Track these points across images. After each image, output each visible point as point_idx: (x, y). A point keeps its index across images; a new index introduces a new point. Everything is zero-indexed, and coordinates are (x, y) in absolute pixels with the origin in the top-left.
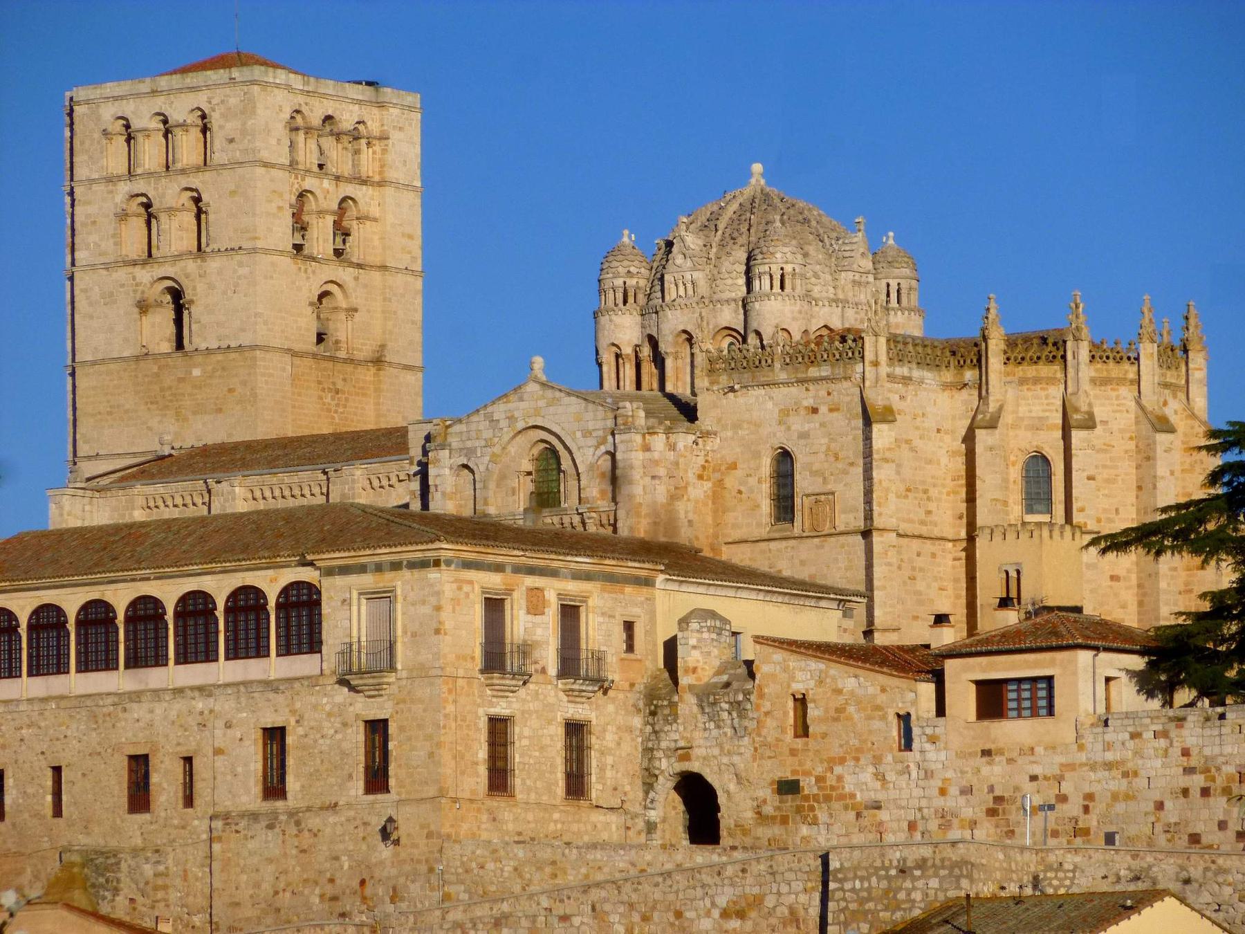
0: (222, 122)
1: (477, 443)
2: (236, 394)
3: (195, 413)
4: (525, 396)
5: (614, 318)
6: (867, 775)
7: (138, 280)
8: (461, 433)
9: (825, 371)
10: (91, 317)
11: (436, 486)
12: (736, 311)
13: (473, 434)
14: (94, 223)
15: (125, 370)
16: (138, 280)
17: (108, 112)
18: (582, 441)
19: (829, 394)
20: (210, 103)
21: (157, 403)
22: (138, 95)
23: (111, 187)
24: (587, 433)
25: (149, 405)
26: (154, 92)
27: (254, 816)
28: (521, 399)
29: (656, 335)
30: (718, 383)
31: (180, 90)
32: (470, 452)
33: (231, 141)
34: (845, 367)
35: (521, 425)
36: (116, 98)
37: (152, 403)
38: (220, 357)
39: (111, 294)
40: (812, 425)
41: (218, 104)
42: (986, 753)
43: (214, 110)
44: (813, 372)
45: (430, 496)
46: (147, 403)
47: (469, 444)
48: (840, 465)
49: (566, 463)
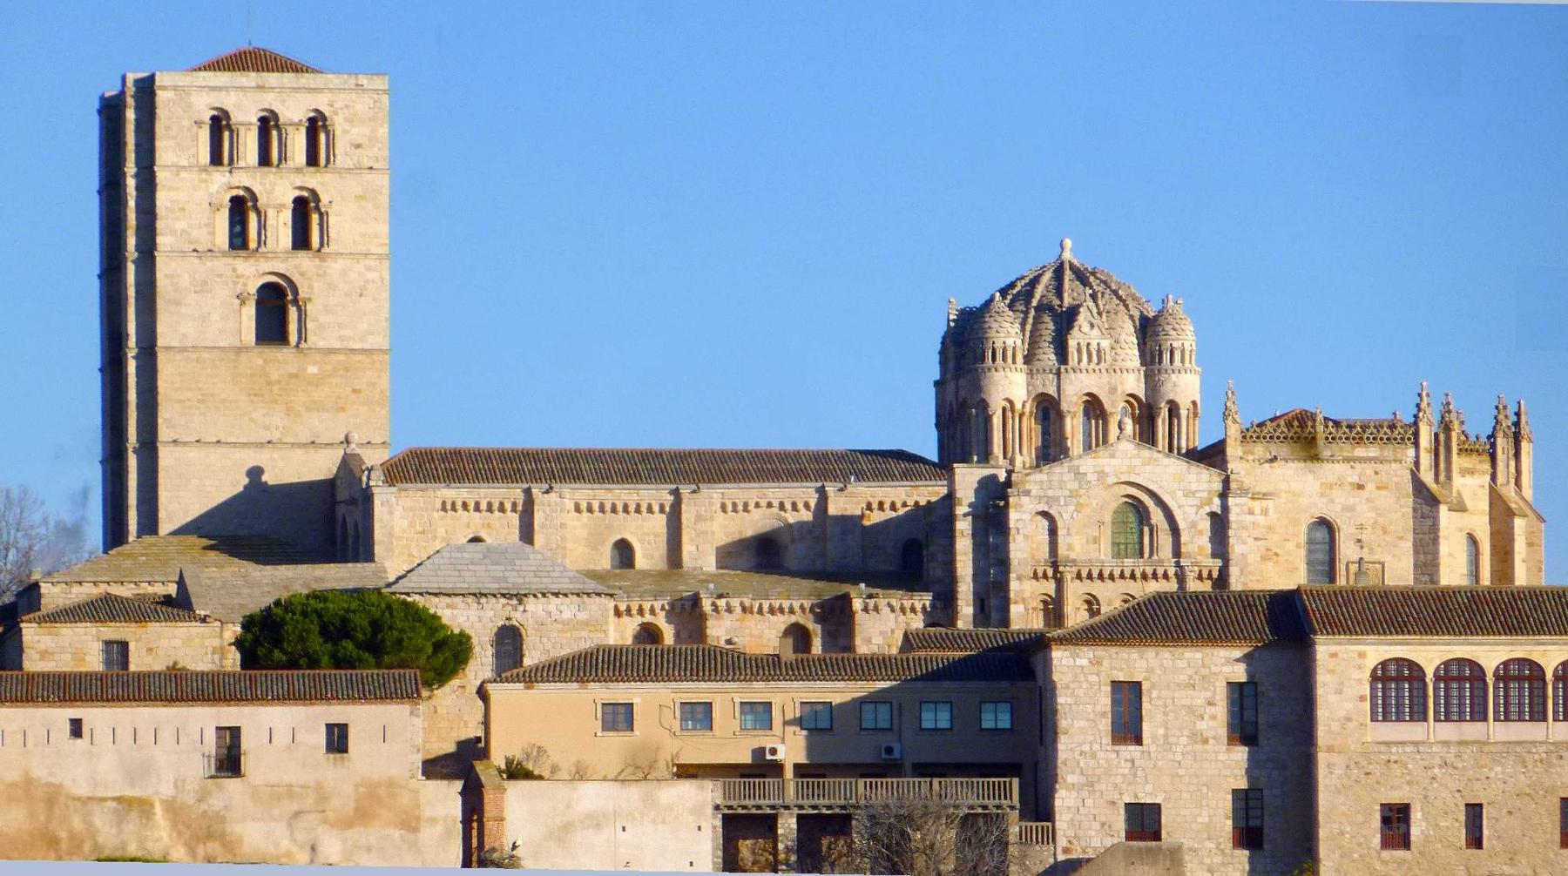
1: (1060, 493)
3: (308, 409)
5: (1009, 374)
7: (239, 272)
8: (1042, 482)
9: (1373, 451)
11: (1018, 529)
12: (1138, 380)
13: (1055, 484)
14: (183, 209)
15: (222, 360)
16: (239, 272)
18: (1183, 501)
19: (1376, 473)
20: (332, 106)
21: (262, 395)
22: (242, 88)
23: (204, 176)
24: (1188, 493)
25: (252, 398)
26: (260, 88)
28: (1112, 456)
29: (1056, 396)
30: (1252, 453)
31: (296, 89)
32: (1051, 500)
33: (358, 146)
34: (1394, 450)
36: (213, 89)
37: (255, 395)
38: (342, 357)
39: (205, 283)
40: (1357, 500)
41: (341, 108)
43: (336, 114)
44: (1360, 452)
45: (1011, 538)
47: (1050, 493)
48: (1388, 538)
49: (1157, 516)
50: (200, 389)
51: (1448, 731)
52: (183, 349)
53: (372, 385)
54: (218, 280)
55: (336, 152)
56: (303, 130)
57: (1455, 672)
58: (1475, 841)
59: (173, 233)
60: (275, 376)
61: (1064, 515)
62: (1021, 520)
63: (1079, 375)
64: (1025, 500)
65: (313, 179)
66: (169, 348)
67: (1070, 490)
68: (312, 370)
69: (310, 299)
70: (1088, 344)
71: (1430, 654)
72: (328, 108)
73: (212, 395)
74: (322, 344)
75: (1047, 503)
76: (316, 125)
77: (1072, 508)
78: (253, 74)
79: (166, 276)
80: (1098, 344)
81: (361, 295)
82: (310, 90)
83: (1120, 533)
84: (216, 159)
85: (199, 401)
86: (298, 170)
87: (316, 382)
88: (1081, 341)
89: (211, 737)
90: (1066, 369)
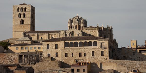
6: (131, 56)
27: (92, 57)
42: (141, 55)
44: (93, 29)
51: (71, 47)
52: (16, 25)
57: (72, 43)
58: (72, 56)
68: (25, 26)
71: (69, 42)
76: (25, 8)
87: (25, 27)
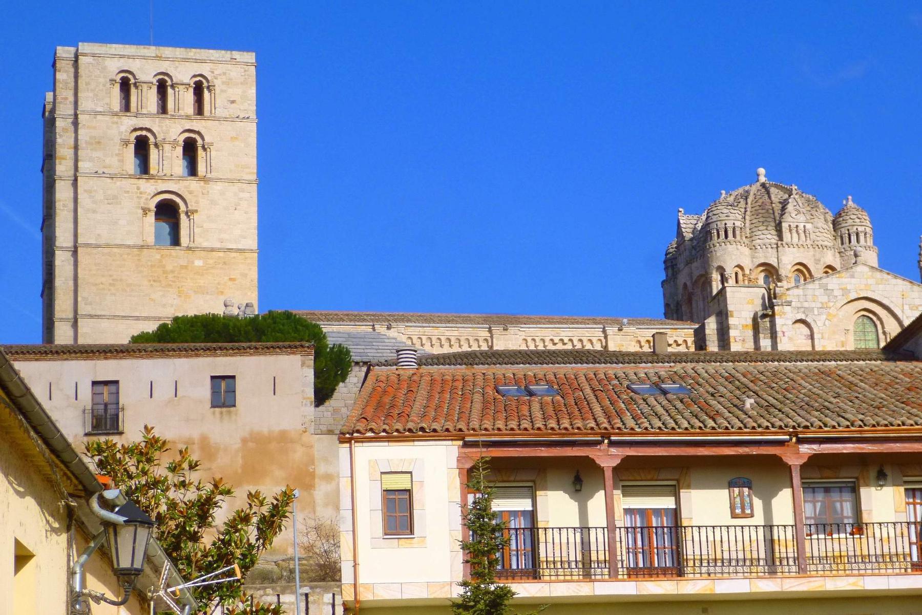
0: (224, 87)
1: (813, 305)
2: (236, 282)
4: (856, 275)
5: (739, 247)
7: (142, 190)
10: (94, 212)
13: (810, 298)
14: (99, 143)
15: (128, 254)
16: (142, 190)
17: (114, 67)
20: (213, 72)
21: (160, 281)
23: (115, 119)
25: (152, 283)
26: (158, 58)
28: (852, 276)
29: (775, 265)
31: (185, 60)
32: (806, 310)
33: (233, 102)
35: (853, 296)
36: (122, 56)
37: (154, 281)
38: (221, 254)
39: (115, 197)
41: (220, 75)
46: (150, 281)
47: (806, 305)
50: (111, 276)
52: (98, 246)
53: (245, 275)
54: (126, 195)
55: (217, 106)
56: (191, 90)
59: (91, 160)
60: (169, 267)
61: (818, 322)
62: (785, 324)
63: (791, 249)
64: (787, 309)
65: (197, 125)
66: (87, 245)
67: (822, 303)
68: (198, 263)
69: (196, 211)
70: (797, 226)
72: (210, 73)
73: (121, 280)
74: (205, 244)
75: (804, 312)
77: (824, 317)
78: (153, 48)
79: (85, 191)
80: (804, 226)
81: (236, 209)
82: (196, 61)
83: (860, 340)
84: (127, 107)
85: (110, 284)
86: (188, 117)
88: (791, 224)
89: (86, 392)
90: (782, 244)
